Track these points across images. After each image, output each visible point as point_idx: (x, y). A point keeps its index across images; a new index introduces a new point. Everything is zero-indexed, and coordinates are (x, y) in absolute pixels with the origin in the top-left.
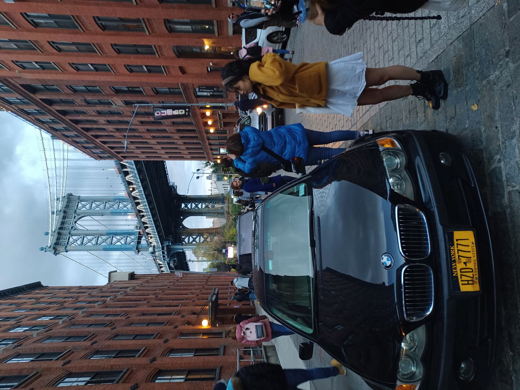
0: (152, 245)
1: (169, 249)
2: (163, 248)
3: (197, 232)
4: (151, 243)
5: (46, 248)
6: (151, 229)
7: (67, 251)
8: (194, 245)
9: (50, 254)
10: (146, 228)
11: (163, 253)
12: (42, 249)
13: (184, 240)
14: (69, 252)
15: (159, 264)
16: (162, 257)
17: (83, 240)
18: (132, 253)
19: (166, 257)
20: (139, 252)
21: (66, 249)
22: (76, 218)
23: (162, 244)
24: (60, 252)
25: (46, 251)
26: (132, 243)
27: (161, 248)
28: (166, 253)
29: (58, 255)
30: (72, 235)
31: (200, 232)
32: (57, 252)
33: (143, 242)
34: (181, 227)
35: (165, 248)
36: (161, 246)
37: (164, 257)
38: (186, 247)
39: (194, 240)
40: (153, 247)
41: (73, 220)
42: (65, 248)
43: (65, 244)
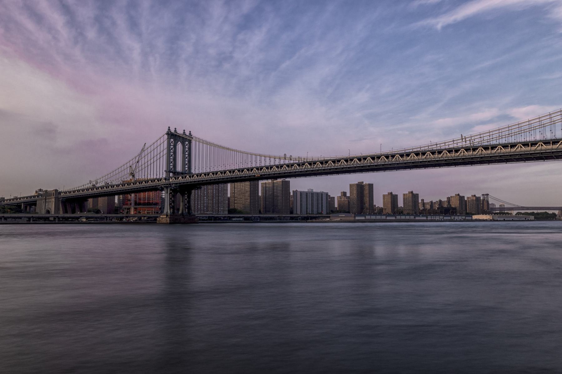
12: (169, 127)
19: (165, 186)
20: (166, 172)
25: (168, 129)
28: (167, 186)
37: (165, 184)
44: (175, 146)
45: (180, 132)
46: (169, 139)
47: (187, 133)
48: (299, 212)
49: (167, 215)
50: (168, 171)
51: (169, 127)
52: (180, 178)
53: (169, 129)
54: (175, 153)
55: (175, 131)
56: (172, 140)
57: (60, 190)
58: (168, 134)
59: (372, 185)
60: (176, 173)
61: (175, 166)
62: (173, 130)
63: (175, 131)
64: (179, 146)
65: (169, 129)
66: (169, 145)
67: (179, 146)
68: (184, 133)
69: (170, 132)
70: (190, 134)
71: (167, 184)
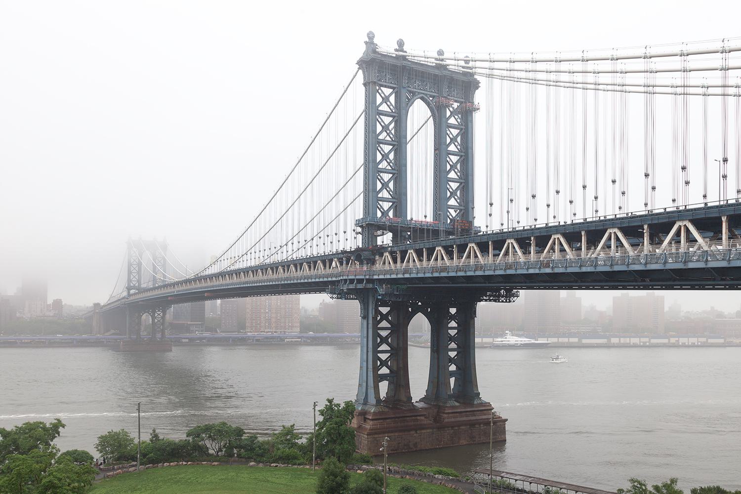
0: (377, 257)
3: (401, 345)
5: (372, 43)
7: (365, 85)
9: (360, 51)
10: (419, 253)
12: (371, 36)
13: (384, 317)
14: (364, 88)
15: (331, 261)
16: (350, 277)
17: (388, 116)
19: (352, 286)
21: (369, 83)
22: (431, 99)
23: (381, 281)
24: (364, 73)
25: (366, 43)
26: (379, 214)
27: (371, 277)
28: (360, 286)
29: (358, 67)
30: (396, 93)
31: (400, 354)
32: (364, 66)
37: (352, 281)
38: (370, 326)
40: (373, 257)
41: (426, 95)
42: (372, 82)
43: (379, 80)
44: (399, 117)
46: (371, 86)
50: (369, 227)
51: (371, 36)
53: (370, 43)
54: (399, 144)
56: (387, 91)
61: (399, 201)
62: (387, 46)
65: (370, 43)
66: (371, 112)
69: (375, 52)
71: (360, 281)
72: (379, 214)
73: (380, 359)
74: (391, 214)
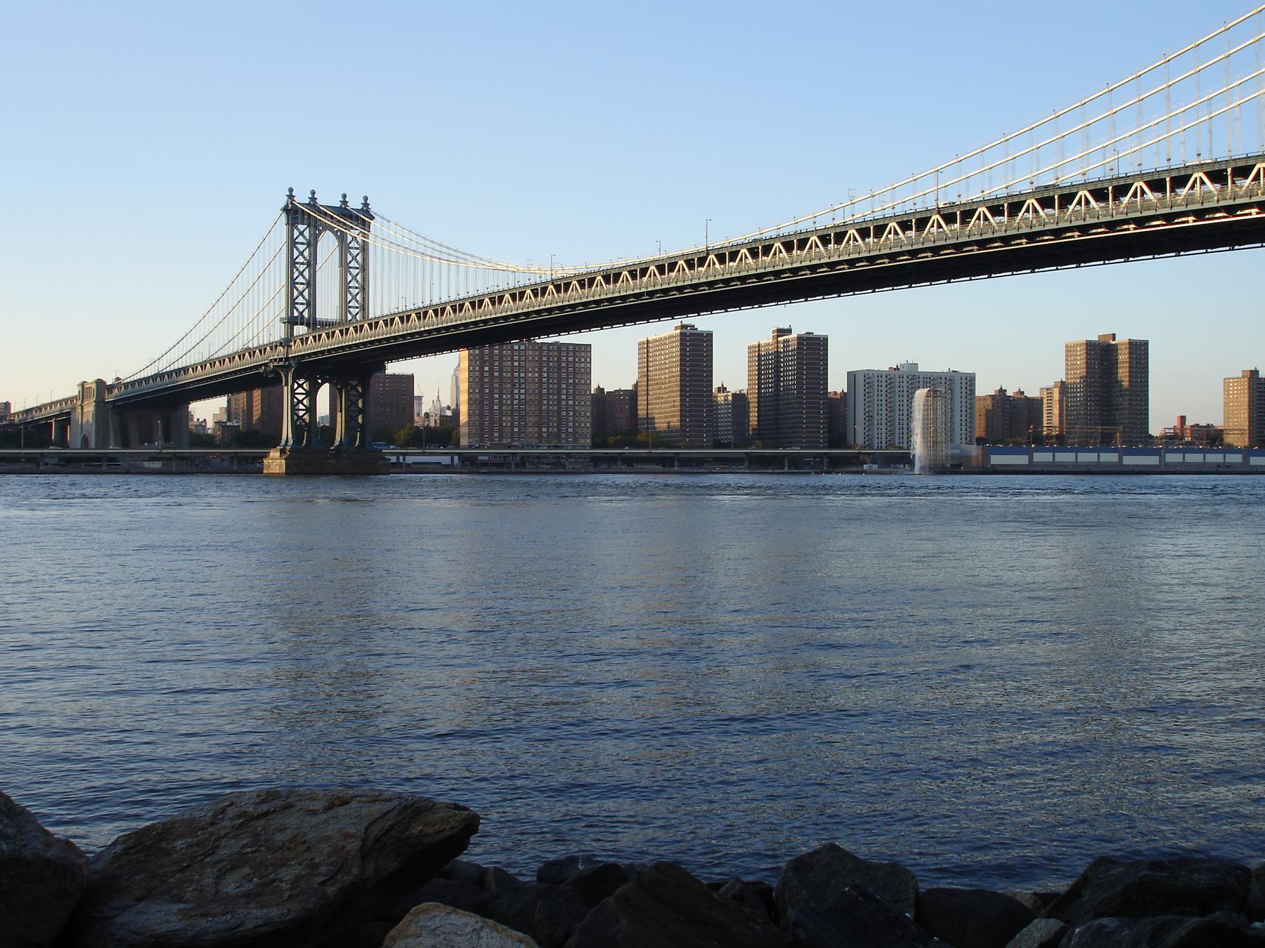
1: (286, 368)
2: (287, 359)
4: (295, 341)
6: (312, 347)
8: (292, 400)
9: (283, 201)
11: (281, 360)
12: (291, 190)
13: (300, 386)
18: (283, 315)
19: (276, 364)
28: (281, 363)
33: (300, 330)
34: (320, 381)
35: (287, 363)
36: (290, 356)
37: (275, 360)
39: (301, 402)
44: (312, 244)
45: (328, 199)
47: (355, 204)
48: (860, 440)
49: (283, 452)
51: (291, 190)
52: (309, 342)
53: (291, 197)
55: (313, 199)
56: (302, 227)
57: (109, 381)
58: (286, 210)
59: (1146, 344)
60: (312, 323)
61: (311, 304)
62: (302, 198)
63: (313, 199)
64: (328, 243)
65: (291, 197)
66: (292, 243)
67: (328, 243)
68: (344, 202)
70: (366, 205)
72: (296, 314)
73: (298, 415)
74: (306, 314)
